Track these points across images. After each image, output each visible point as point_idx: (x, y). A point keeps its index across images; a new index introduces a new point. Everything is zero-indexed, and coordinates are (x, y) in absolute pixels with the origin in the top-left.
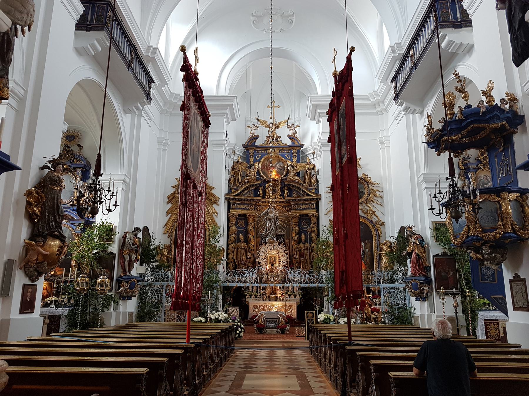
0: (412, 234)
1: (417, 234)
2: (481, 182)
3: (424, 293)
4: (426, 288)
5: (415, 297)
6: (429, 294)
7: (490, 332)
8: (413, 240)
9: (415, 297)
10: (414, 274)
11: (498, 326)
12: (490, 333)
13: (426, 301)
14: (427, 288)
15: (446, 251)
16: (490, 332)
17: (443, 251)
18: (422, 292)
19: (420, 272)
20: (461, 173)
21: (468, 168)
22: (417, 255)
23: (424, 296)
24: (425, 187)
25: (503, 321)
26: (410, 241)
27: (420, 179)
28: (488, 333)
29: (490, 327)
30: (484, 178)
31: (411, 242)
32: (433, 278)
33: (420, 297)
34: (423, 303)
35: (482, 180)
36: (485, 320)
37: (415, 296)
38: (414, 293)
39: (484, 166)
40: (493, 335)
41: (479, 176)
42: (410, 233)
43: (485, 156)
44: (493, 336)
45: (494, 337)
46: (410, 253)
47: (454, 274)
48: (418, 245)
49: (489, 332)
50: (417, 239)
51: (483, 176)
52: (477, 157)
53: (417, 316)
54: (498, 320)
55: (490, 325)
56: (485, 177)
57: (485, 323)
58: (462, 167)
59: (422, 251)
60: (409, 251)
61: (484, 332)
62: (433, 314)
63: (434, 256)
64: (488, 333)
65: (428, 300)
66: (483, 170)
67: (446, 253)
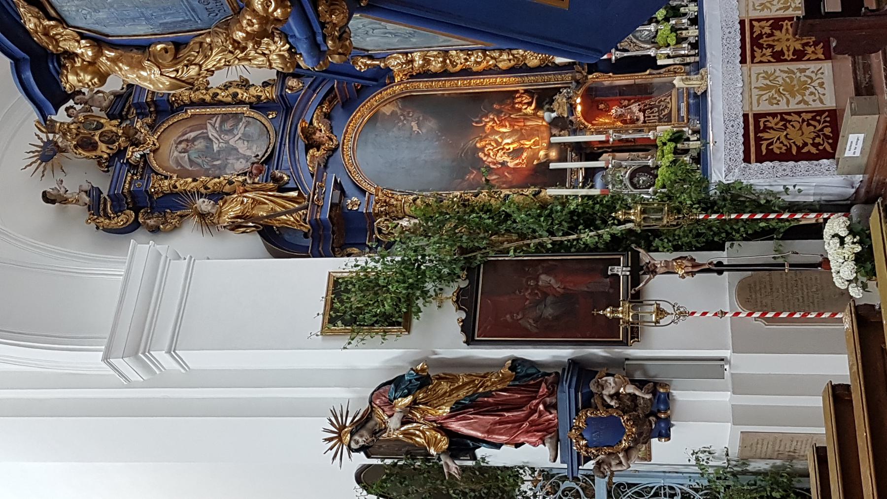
0: (370, 425)
1: (370, 403)
2: (200, 161)
3: (634, 397)
4: (611, 385)
5: (654, 441)
6: (638, 376)
7: (800, 144)
8: (394, 423)
9: (654, 441)
10: (547, 431)
11: (774, 115)
12: (805, 144)
13: (668, 395)
14: (611, 379)
15: (450, 291)
16: (800, 144)
17: (450, 306)
18: (629, 404)
19: (538, 404)
20: (151, 222)
21: (133, 198)
22: (458, 410)
23: (648, 396)
24: (169, 352)
25: (747, 96)
26: (397, 440)
27: (134, 377)
28: (804, 150)
29: (778, 144)
30: (185, 151)
31: (405, 433)
32: (565, 353)
33: (652, 419)
34: (677, 411)
35: (193, 157)
36: (747, 159)
37: (647, 441)
38: (636, 441)
39: (136, 144)
40: (813, 135)
41: (174, 166)
42: (364, 432)
43: (97, 138)
44: (819, 136)
45: (821, 130)
46: (451, 443)
47: (551, 268)
48: (415, 402)
49: (799, 149)
50: (390, 403)
51: (176, 154)
52: (100, 164)
53: (743, 440)
54: (746, 116)
55: (771, 144)
56: (183, 145)
57: (760, 159)
58: (123, 217)
59: (445, 386)
60: (444, 444)
61: (803, 164)
62: (727, 367)
63: (470, 341)
64: (804, 150)
65: (665, 385)
66: (154, 151)
67: (461, 292)
